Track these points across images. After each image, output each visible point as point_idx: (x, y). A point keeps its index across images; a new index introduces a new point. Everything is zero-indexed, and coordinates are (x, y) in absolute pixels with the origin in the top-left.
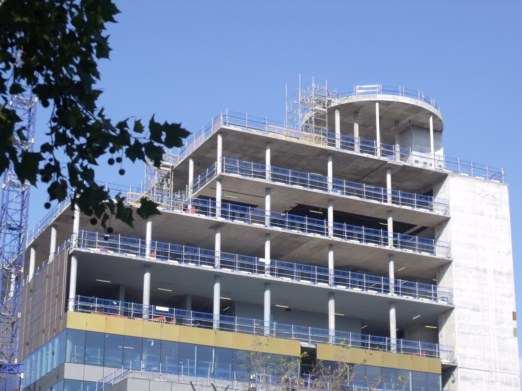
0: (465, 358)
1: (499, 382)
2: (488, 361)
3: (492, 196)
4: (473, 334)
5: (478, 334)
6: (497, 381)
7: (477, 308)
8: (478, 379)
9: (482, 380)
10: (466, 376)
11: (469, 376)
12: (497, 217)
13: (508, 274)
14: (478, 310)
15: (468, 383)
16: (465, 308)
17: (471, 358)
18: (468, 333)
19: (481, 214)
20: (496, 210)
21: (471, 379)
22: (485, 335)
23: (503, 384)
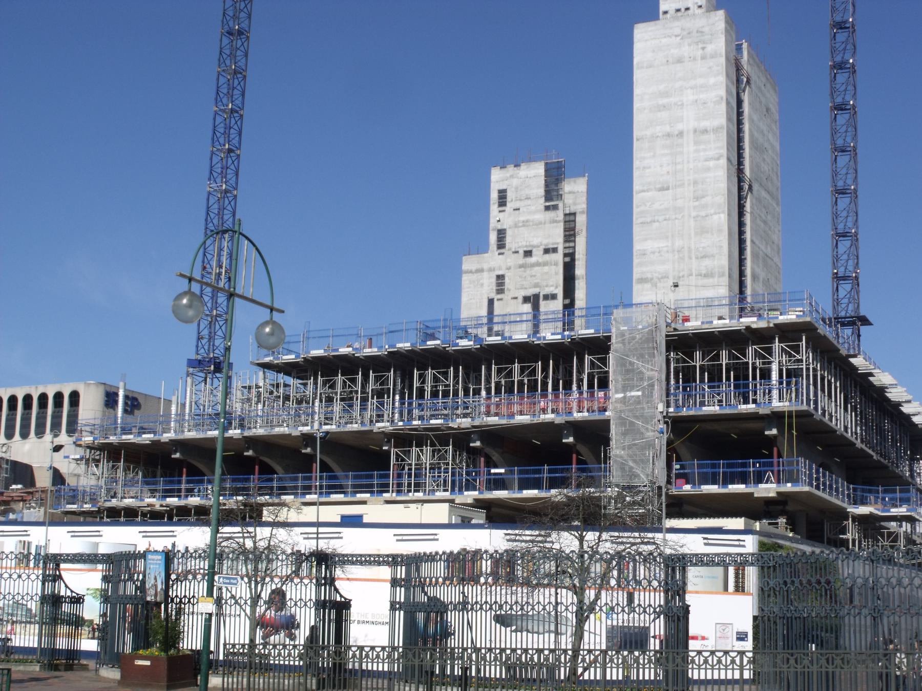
0: (644, 254)
1: (694, 274)
2: (679, 251)
3: (697, 32)
4: (658, 221)
5: (665, 220)
6: (691, 275)
7: (665, 186)
8: (662, 278)
9: (668, 277)
10: (644, 277)
11: (649, 276)
12: (703, 58)
13: (716, 130)
14: (668, 189)
15: (648, 286)
16: (648, 191)
17: (653, 253)
18: (651, 222)
19: (680, 61)
20: (703, 49)
21: (652, 279)
22: (676, 219)
23: (700, 277)
